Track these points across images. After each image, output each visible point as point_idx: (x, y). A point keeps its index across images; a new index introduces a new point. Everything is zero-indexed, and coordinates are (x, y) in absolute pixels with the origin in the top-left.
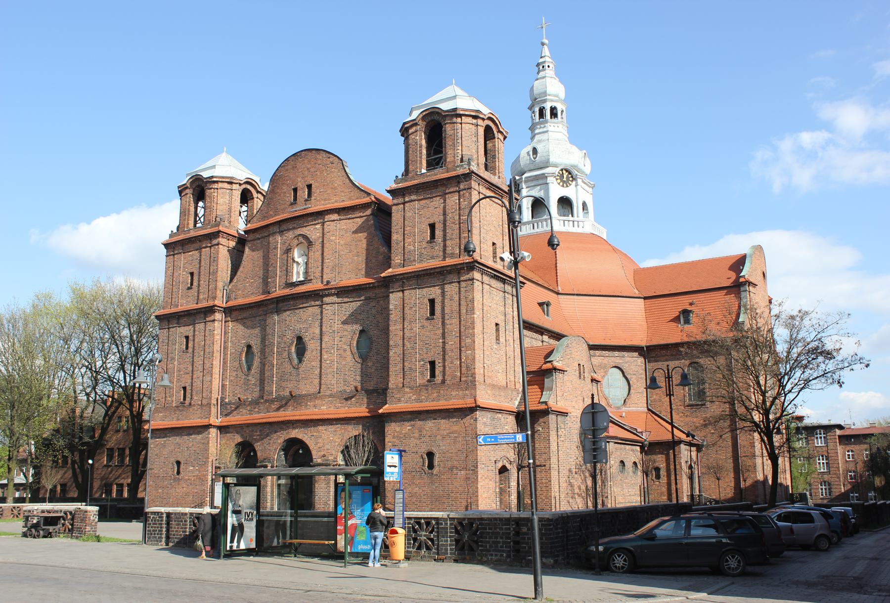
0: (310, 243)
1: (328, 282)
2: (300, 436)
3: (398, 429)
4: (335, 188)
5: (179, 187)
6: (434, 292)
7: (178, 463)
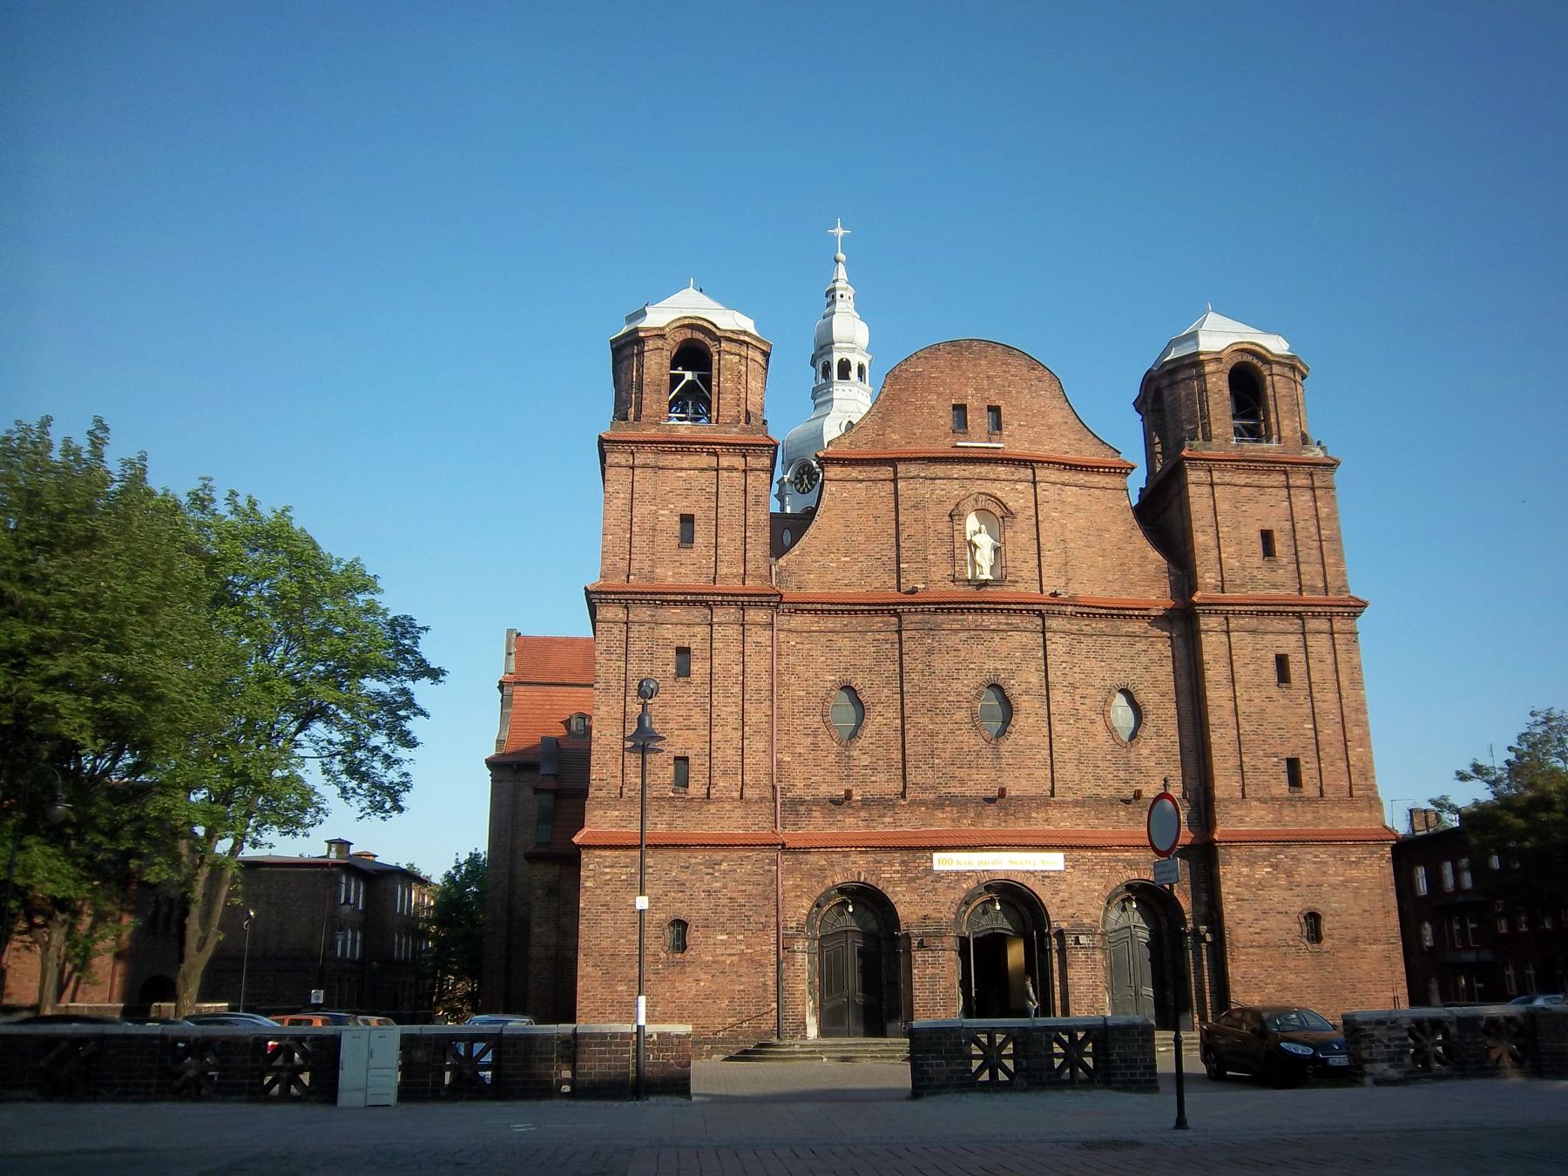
0: (1009, 514)
1: (1055, 595)
3: (1245, 870)
7: (680, 925)
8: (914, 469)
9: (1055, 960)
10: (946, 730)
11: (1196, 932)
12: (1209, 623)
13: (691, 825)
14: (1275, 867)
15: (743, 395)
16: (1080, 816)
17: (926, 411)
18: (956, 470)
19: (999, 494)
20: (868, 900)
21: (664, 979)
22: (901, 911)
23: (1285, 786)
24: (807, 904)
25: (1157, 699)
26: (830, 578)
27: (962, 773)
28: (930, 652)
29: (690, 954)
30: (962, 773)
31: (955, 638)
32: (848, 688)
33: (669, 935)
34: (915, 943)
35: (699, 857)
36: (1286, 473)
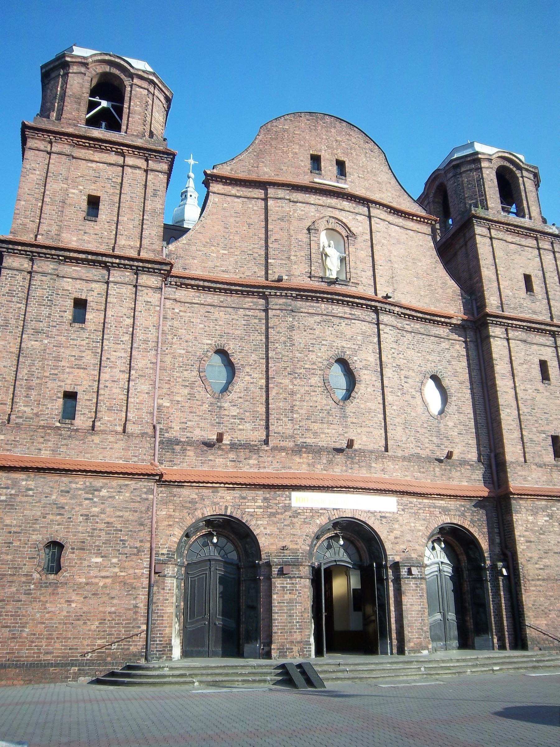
0: (351, 235)
3: (531, 518)
4: (379, 183)
7: (56, 547)
8: (281, 193)
9: (391, 588)
10: (302, 390)
11: (494, 567)
12: (495, 331)
13: (72, 454)
14: (551, 516)
15: (148, 119)
16: (407, 469)
17: (290, 155)
18: (313, 198)
19: (344, 220)
20: (232, 531)
21: (35, 600)
22: (263, 542)
24: (178, 533)
25: (458, 386)
26: (210, 264)
27: (316, 427)
28: (291, 328)
29: (63, 576)
30: (316, 427)
31: (311, 321)
32: (222, 352)
33: (44, 556)
34: (275, 570)
35: (80, 482)
36: (536, 239)
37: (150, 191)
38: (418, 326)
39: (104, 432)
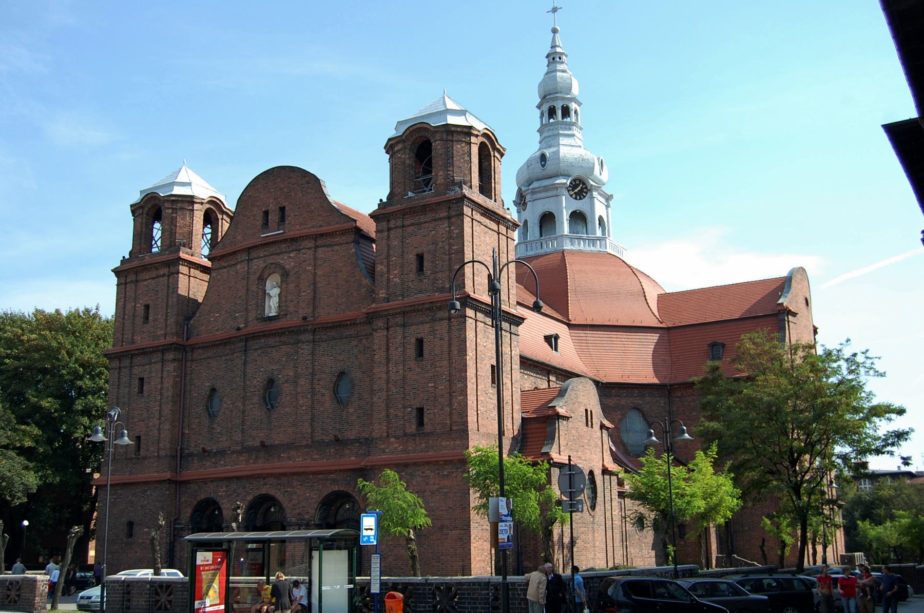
2: (272, 492)
5: (131, 206)
6: (423, 330)
7: (131, 524)
23: (414, 427)
37: (171, 290)
38: (333, 333)
39: (150, 458)
